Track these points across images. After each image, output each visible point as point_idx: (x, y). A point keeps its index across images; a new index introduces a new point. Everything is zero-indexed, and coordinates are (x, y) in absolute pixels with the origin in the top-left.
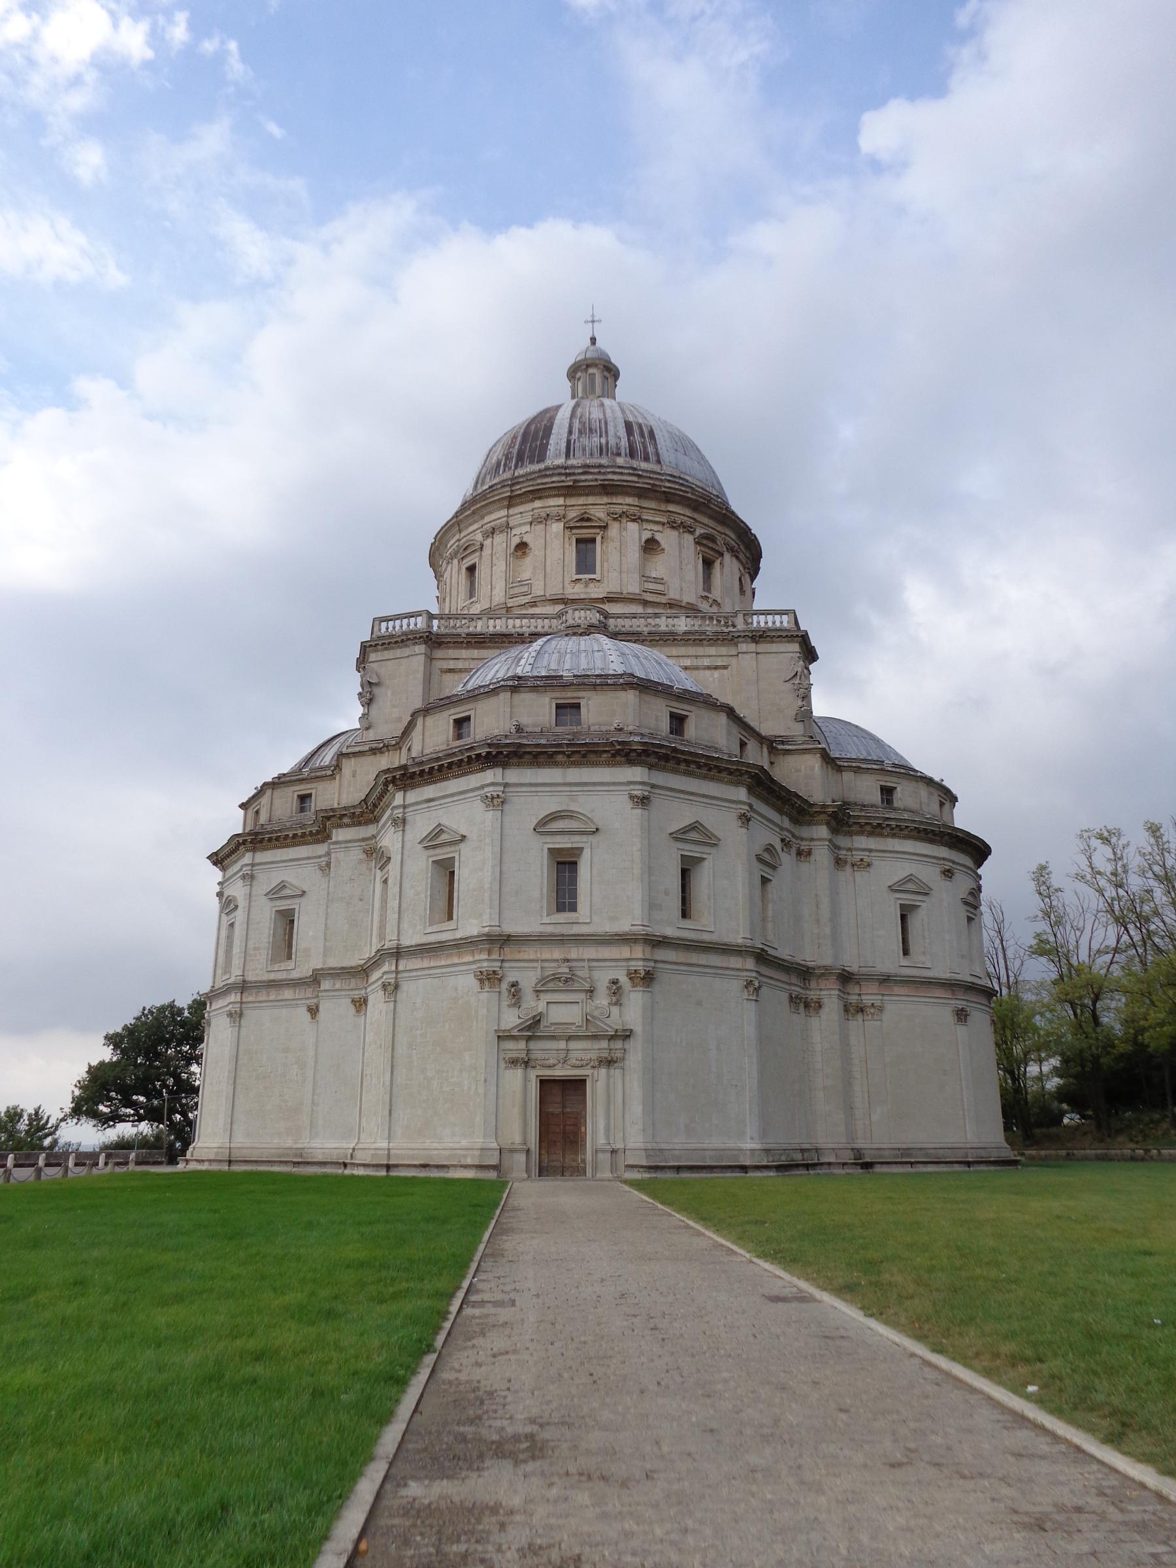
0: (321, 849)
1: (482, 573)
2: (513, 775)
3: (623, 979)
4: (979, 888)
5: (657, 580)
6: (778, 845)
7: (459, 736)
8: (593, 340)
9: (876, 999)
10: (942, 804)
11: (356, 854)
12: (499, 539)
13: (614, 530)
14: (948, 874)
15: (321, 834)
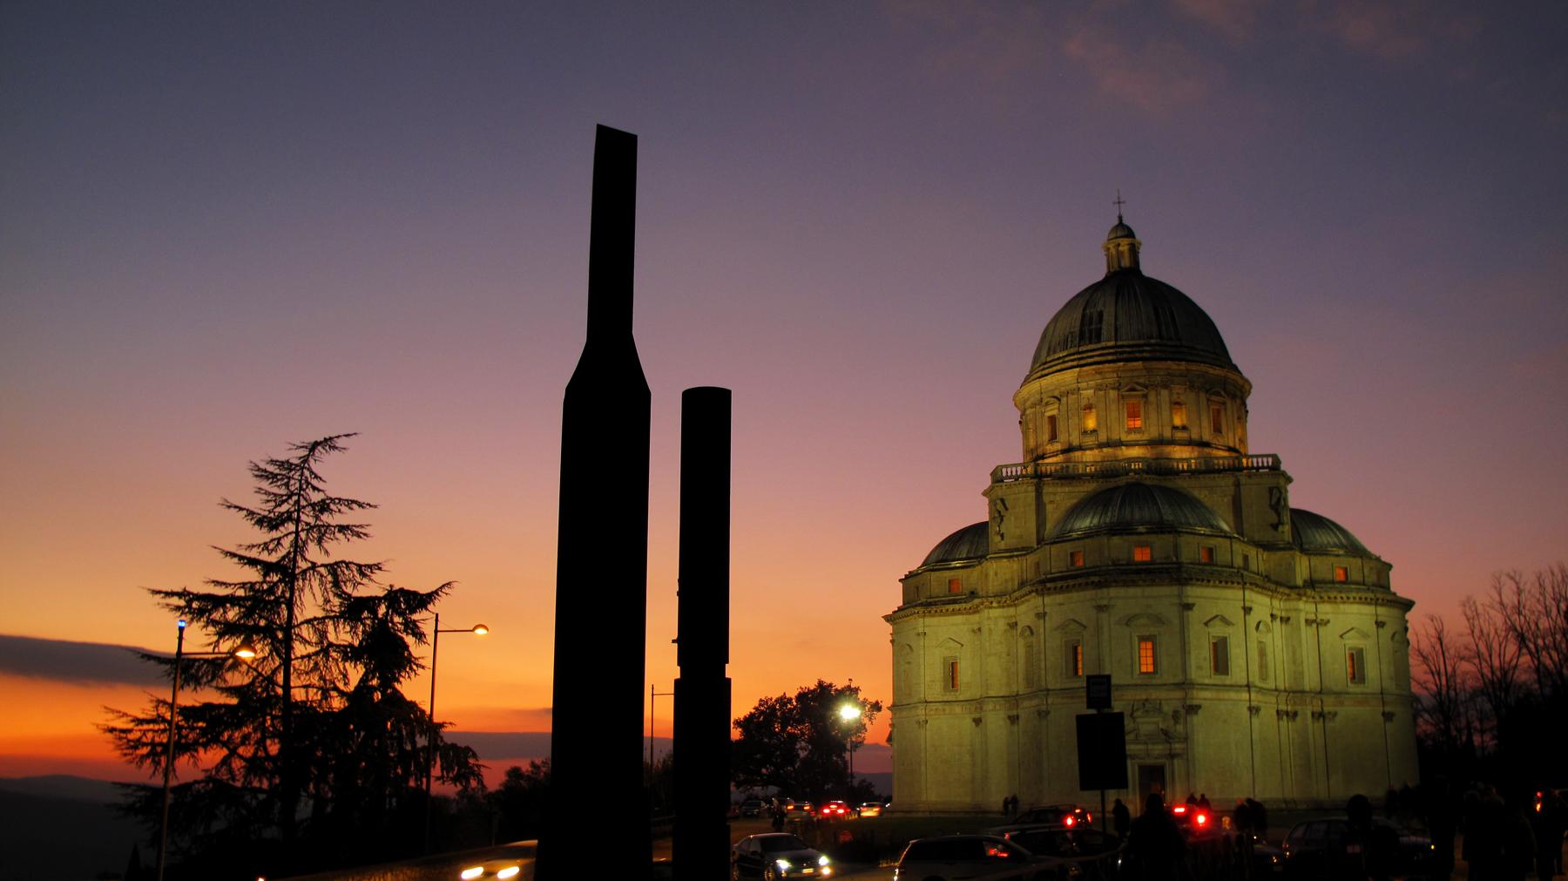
0: (976, 617)
1: (1061, 425)
2: (1113, 591)
3: (1183, 711)
4: (1406, 629)
5: (1184, 428)
6: (1269, 619)
7: (1073, 563)
8: (1120, 218)
9: (1331, 709)
10: (1379, 574)
11: (1002, 625)
12: (1072, 398)
13: (1152, 397)
14: (1380, 624)
15: (976, 611)
